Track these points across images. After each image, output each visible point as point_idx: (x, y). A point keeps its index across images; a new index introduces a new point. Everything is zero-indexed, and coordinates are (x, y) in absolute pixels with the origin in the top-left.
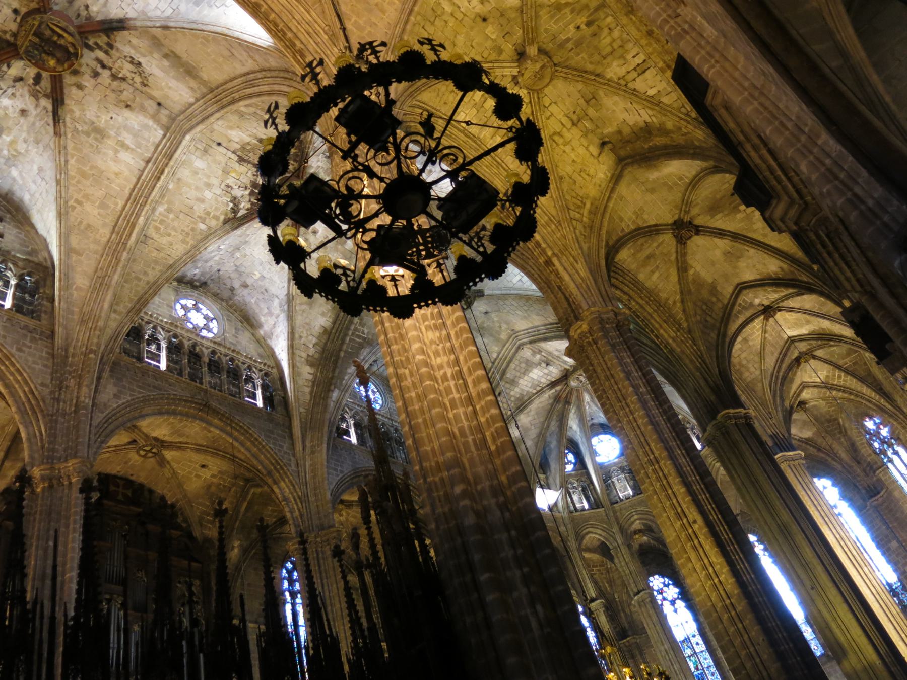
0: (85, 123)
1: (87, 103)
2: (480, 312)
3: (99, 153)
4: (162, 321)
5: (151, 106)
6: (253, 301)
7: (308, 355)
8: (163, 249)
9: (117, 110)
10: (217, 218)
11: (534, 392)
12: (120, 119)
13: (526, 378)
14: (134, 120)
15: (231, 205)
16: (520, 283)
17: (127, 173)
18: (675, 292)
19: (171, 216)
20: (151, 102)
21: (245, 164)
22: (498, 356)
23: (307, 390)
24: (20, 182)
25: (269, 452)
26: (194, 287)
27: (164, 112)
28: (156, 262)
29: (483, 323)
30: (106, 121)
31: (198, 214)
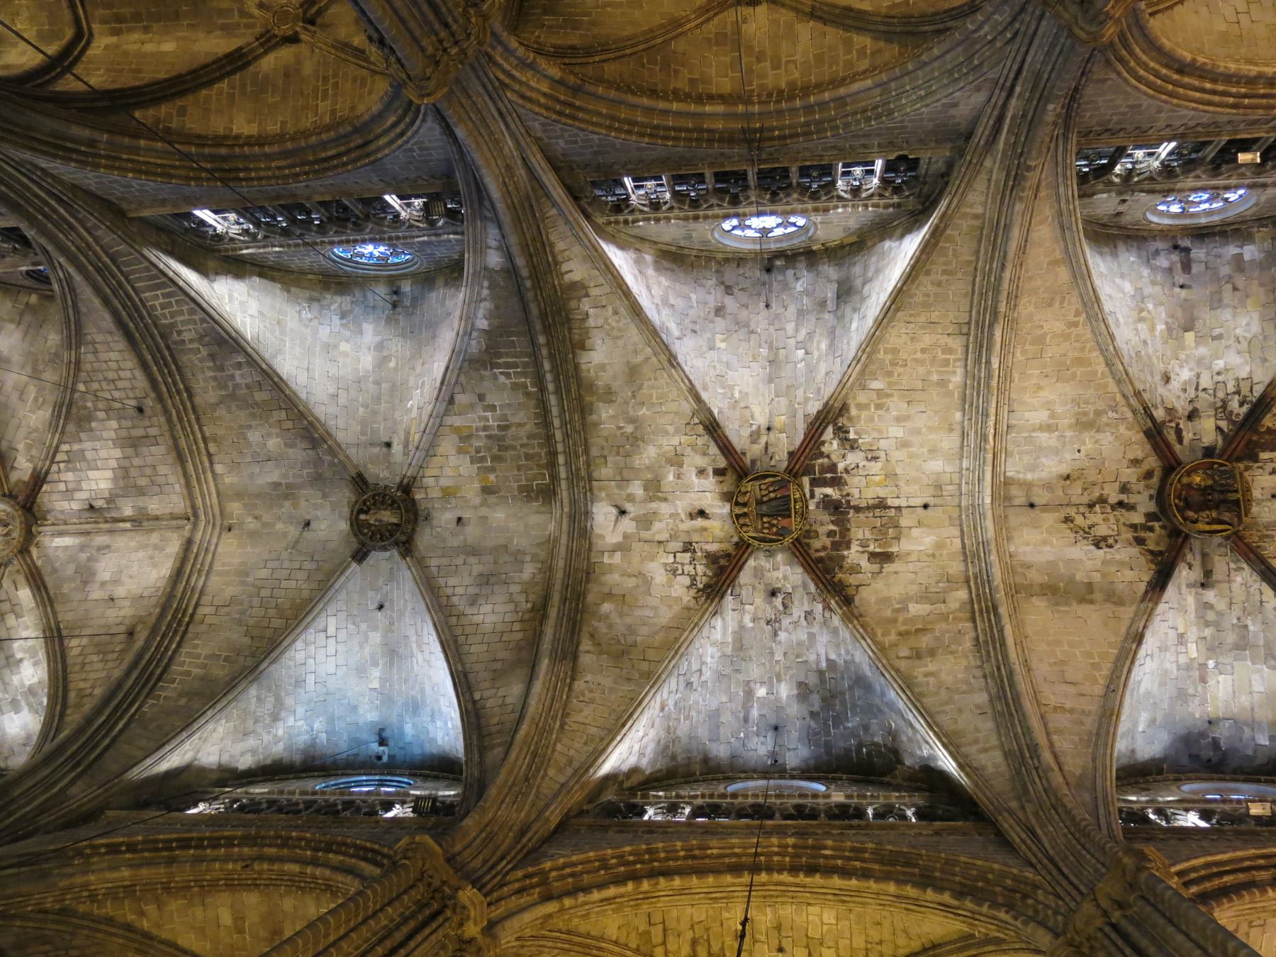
0: (1107, 425)
1: (1117, 450)
2: (317, 518)
3: (1073, 400)
4: (844, 206)
5: (1041, 497)
6: (693, 297)
7: (587, 295)
8: (923, 328)
9: (1078, 465)
10: (860, 407)
11: (65, 447)
12: (1068, 456)
13: (113, 464)
14: (1052, 467)
15: (852, 436)
16: (321, 627)
17: (1027, 398)
18: (159, 926)
19: (935, 377)
20: (1043, 501)
21: (871, 502)
22: (213, 471)
23: (560, 246)
24: (1118, 280)
25: (593, 124)
26: (780, 254)
27: (1020, 499)
28: (926, 305)
29: (295, 506)
30: (1084, 443)
31: (896, 399)
